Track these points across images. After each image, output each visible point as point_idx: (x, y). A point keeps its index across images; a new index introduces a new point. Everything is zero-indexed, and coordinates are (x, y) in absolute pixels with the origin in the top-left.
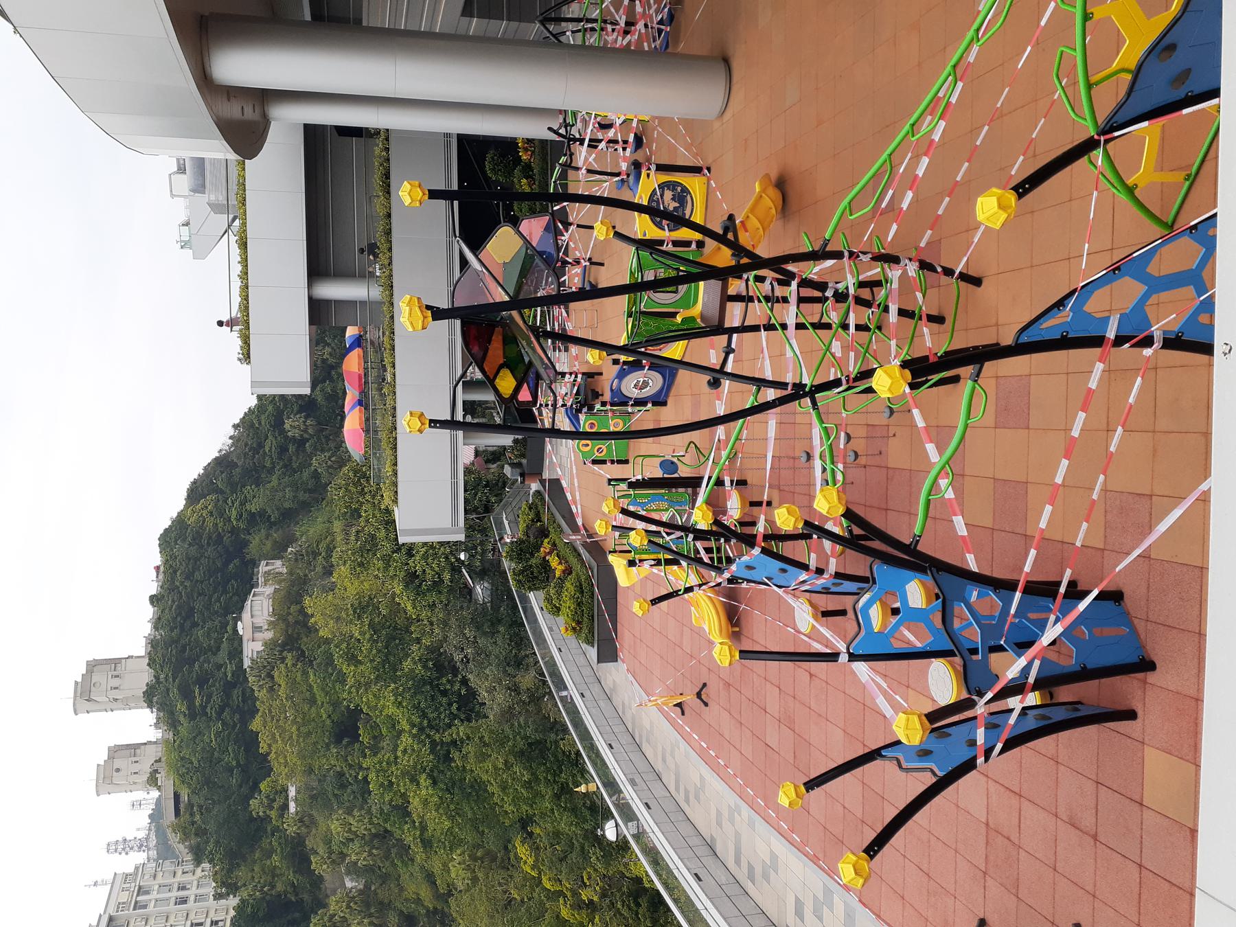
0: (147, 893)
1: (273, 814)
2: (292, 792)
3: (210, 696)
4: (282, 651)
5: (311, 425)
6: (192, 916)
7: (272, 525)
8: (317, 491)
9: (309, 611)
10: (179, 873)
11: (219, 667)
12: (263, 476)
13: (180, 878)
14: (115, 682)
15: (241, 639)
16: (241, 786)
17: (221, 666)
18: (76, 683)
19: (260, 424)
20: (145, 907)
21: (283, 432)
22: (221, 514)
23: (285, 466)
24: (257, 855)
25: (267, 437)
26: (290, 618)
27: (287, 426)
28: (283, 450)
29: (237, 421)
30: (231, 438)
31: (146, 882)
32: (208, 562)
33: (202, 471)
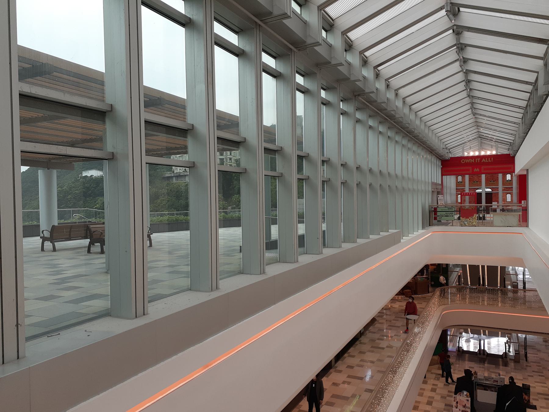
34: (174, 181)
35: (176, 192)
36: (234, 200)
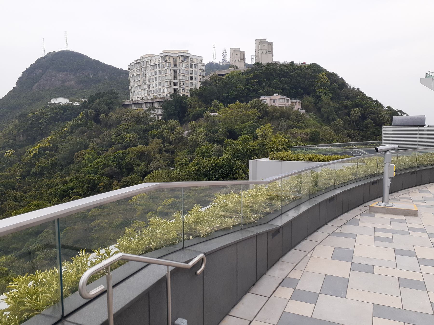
0: (195, 67)
1: (212, 108)
2: (216, 114)
3: (254, 85)
4: (263, 111)
5: (356, 118)
6: (187, 82)
7: (315, 104)
8: (328, 121)
9: (266, 125)
10: (200, 77)
11: (263, 88)
12: (336, 100)
13: (199, 77)
14: (264, 52)
15: (272, 95)
16: (222, 97)
17: (264, 88)
18: (266, 39)
19: (358, 99)
20: (191, 67)
21: (353, 107)
22: (321, 86)
23: (339, 108)
24: (200, 103)
25: (352, 101)
26: (275, 113)
27: (355, 109)
28: (346, 107)
29: (360, 90)
30: (353, 87)
31: (199, 67)
32: (303, 82)
33: (340, 78)
34: (133, 107)
35: (136, 118)
36: (191, 126)
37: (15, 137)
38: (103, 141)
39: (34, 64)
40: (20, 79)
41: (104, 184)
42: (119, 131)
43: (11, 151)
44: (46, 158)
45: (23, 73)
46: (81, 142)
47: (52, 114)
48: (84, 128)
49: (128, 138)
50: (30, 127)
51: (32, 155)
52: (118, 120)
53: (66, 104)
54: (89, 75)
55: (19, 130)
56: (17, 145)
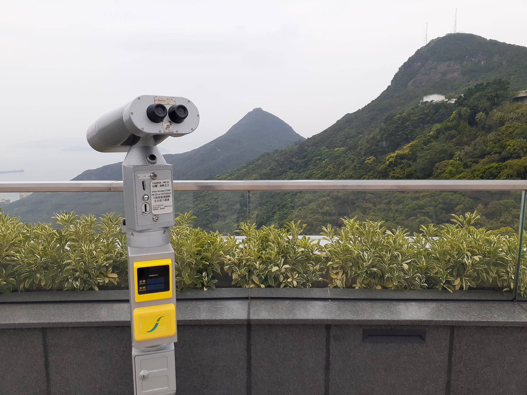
37: (378, 142)
38: (474, 150)
39: (412, 57)
40: (397, 75)
41: (464, 207)
42: (499, 135)
43: (372, 158)
44: (402, 168)
45: (399, 68)
46: (446, 150)
47: (421, 115)
48: (453, 132)
49: (511, 146)
50: (394, 131)
51: (387, 163)
52: (500, 121)
53: (440, 101)
54: (480, 61)
55: (383, 134)
56: (379, 152)
